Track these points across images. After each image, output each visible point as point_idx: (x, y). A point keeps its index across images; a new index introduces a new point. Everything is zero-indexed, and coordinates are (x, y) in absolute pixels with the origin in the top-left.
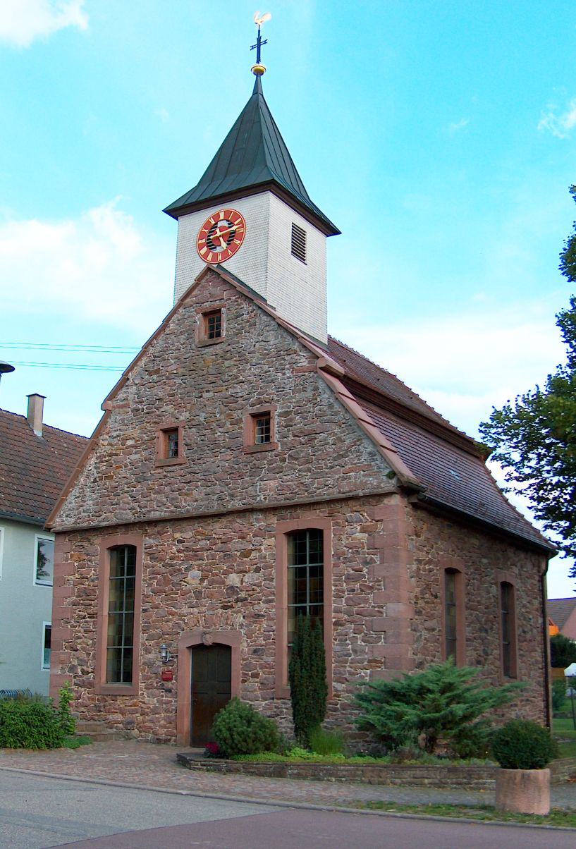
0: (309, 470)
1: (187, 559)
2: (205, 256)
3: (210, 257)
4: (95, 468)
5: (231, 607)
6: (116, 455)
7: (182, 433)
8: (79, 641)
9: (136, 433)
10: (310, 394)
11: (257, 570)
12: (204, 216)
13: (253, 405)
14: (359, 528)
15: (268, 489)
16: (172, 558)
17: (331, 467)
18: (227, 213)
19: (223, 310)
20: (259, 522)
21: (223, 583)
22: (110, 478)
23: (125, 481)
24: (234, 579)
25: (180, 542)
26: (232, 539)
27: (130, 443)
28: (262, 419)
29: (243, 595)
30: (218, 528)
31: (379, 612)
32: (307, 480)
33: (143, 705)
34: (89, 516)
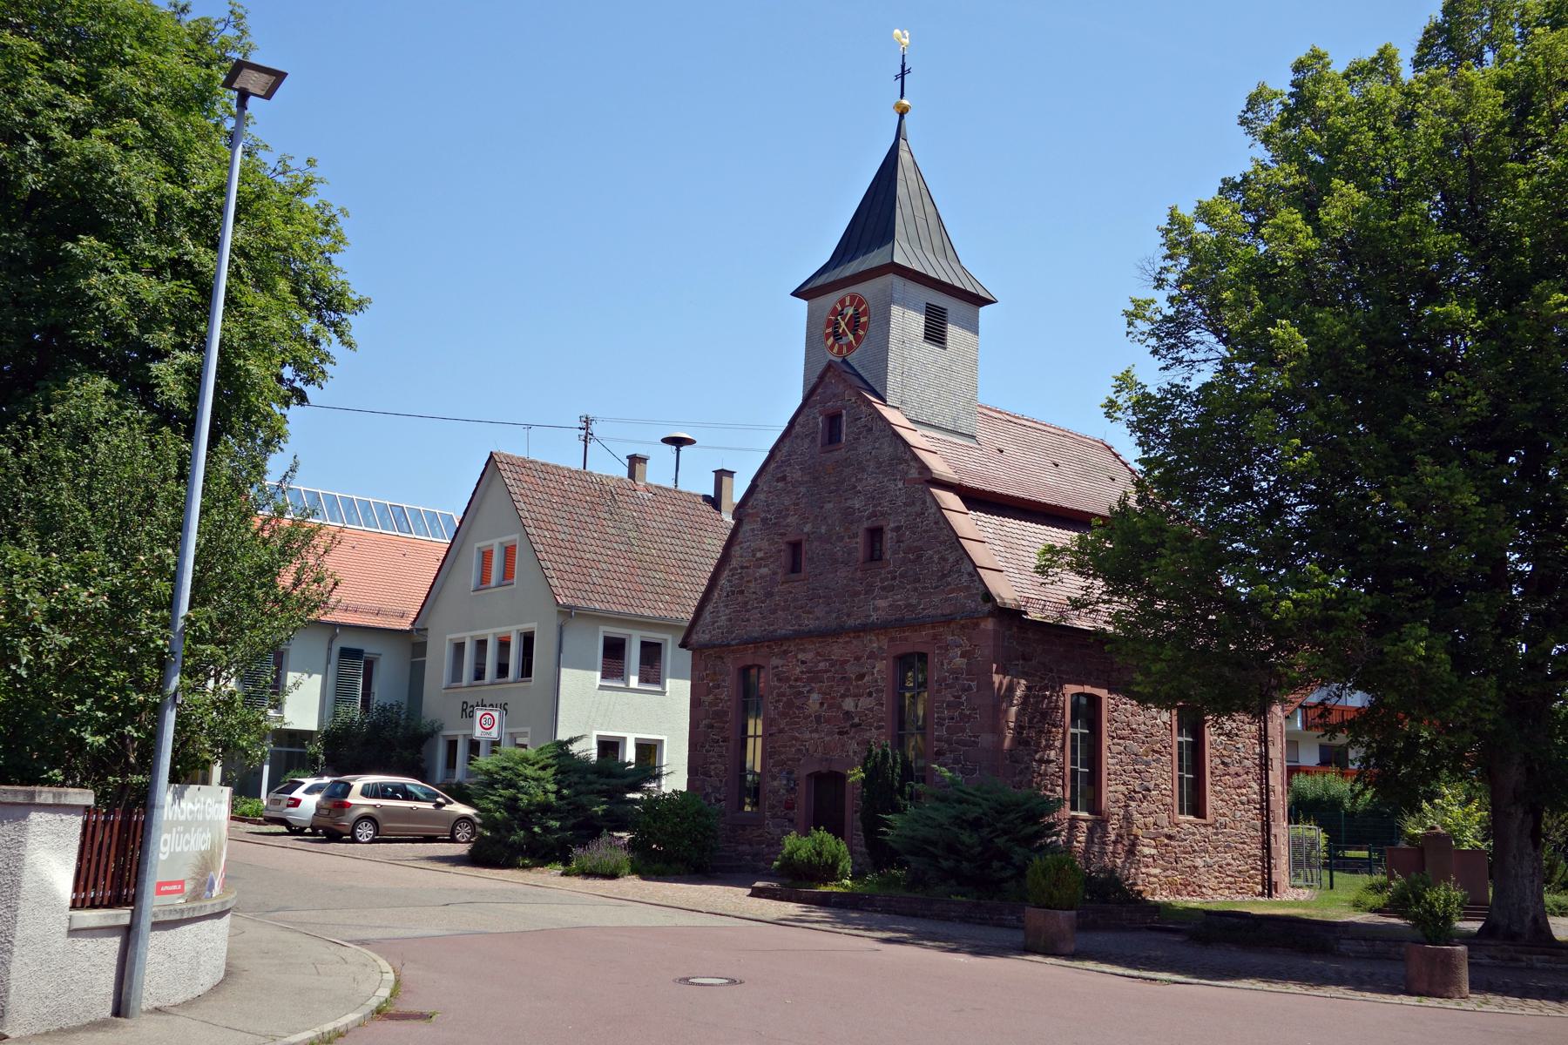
0: (916, 589)
1: (810, 680)
2: (832, 347)
3: (836, 350)
4: (729, 581)
5: (847, 733)
6: (747, 567)
7: (805, 546)
8: (713, 767)
9: (765, 545)
10: (918, 508)
11: (870, 694)
12: (831, 300)
13: (868, 518)
14: (959, 653)
15: (880, 607)
16: (796, 680)
17: (937, 587)
18: (853, 298)
19: (844, 412)
20: (874, 643)
21: (840, 707)
22: (742, 592)
23: (754, 596)
24: (848, 704)
25: (803, 662)
26: (849, 661)
27: (759, 555)
28: (875, 534)
29: (856, 720)
30: (837, 650)
31: (974, 742)
32: (914, 601)
33: (769, 836)
34: (722, 633)
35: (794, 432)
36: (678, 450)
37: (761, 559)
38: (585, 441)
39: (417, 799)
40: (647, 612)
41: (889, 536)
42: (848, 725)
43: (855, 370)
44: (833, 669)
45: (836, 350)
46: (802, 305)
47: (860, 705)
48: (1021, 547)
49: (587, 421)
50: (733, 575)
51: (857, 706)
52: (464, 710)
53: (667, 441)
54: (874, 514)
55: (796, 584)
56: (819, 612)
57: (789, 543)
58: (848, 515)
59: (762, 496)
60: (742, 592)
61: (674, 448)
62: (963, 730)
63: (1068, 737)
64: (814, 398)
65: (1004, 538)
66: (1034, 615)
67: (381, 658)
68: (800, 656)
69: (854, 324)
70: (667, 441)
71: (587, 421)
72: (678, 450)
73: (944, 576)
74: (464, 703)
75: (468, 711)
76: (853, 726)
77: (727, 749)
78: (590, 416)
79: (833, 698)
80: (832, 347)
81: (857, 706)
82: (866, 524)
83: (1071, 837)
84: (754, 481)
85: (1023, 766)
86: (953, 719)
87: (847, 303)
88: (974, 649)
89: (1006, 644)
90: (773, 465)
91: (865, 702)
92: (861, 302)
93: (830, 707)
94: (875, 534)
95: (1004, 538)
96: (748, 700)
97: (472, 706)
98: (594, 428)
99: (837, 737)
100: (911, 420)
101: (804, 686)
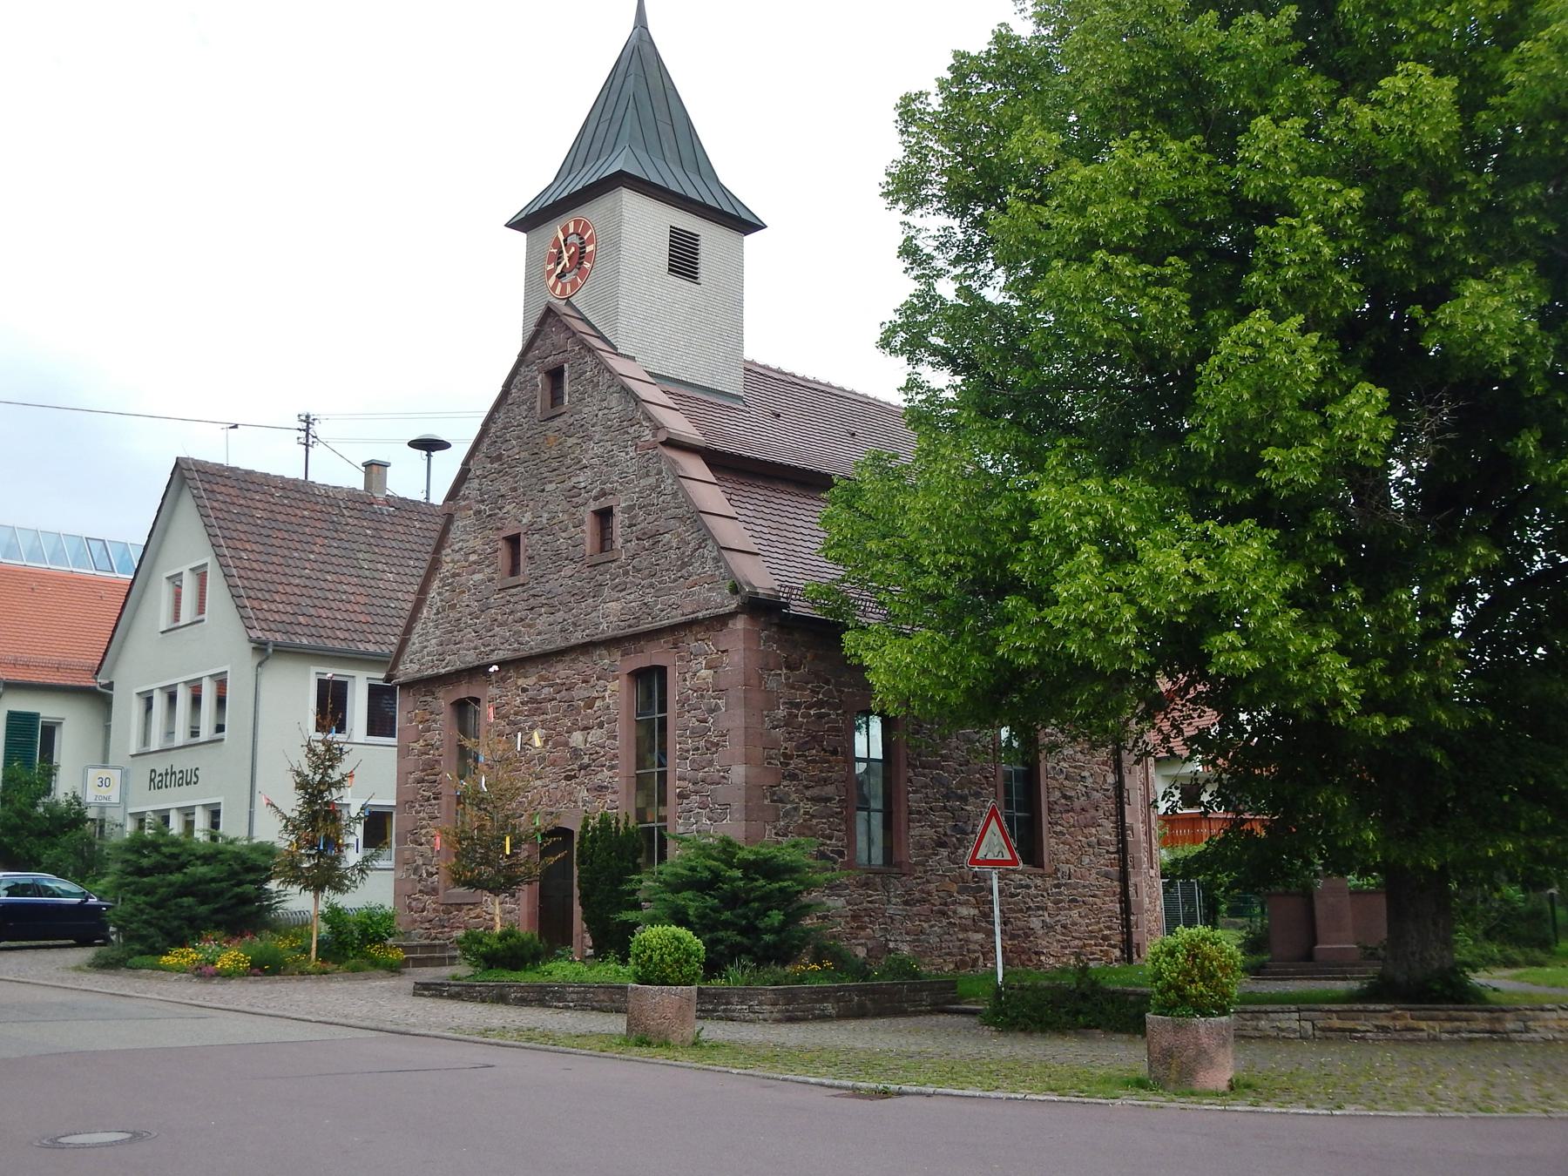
0: (651, 586)
1: (532, 713)
2: (554, 288)
3: (558, 291)
4: (439, 594)
5: (575, 777)
6: (458, 575)
7: (524, 541)
8: (424, 831)
9: (477, 543)
10: (652, 480)
11: (601, 726)
12: (556, 230)
13: (596, 499)
14: (704, 662)
15: (610, 615)
16: (516, 714)
17: (675, 580)
18: (577, 223)
19: (566, 365)
20: (605, 660)
21: (566, 744)
22: (453, 607)
23: (468, 610)
24: (577, 738)
25: (524, 690)
26: (576, 684)
27: (473, 558)
28: (604, 516)
29: (586, 760)
30: (562, 671)
31: (723, 777)
32: (648, 599)
33: (488, 917)
34: (433, 661)
35: (510, 397)
36: (429, 456)
37: (474, 563)
38: (307, 445)
39: (59, 896)
40: (371, 648)
41: (619, 519)
42: (576, 767)
43: (581, 314)
44: (558, 696)
45: (558, 291)
46: (520, 238)
47: (589, 740)
48: (793, 528)
49: (308, 420)
50: (444, 586)
51: (586, 741)
52: (152, 780)
53: (417, 444)
54: (603, 494)
55: (513, 591)
56: (542, 623)
57: (507, 539)
58: (572, 493)
59: (475, 484)
60: (453, 607)
61: (425, 453)
62: (710, 763)
63: (387, 659)
64: (530, 354)
65: (769, 517)
66: (799, 608)
67: (65, 724)
68: (520, 682)
69: (580, 257)
70: (417, 444)
71: (308, 420)
72: (429, 456)
73: (684, 565)
74: (153, 771)
75: (156, 781)
76: (582, 767)
77: (439, 808)
78: (313, 412)
79: (559, 734)
80: (554, 288)
81: (586, 741)
82: (594, 506)
83: (189, 826)
84: (466, 463)
85: (789, 806)
86: (698, 749)
87: (571, 231)
88: (721, 657)
89: (762, 648)
90: (487, 441)
91: (595, 735)
92: (586, 227)
93: (555, 746)
94: (604, 516)
95: (769, 517)
96: (341, 720)
97: (161, 775)
98: (316, 429)
99: (564, 783)
100: (651, 374)
101: (525, 721)
